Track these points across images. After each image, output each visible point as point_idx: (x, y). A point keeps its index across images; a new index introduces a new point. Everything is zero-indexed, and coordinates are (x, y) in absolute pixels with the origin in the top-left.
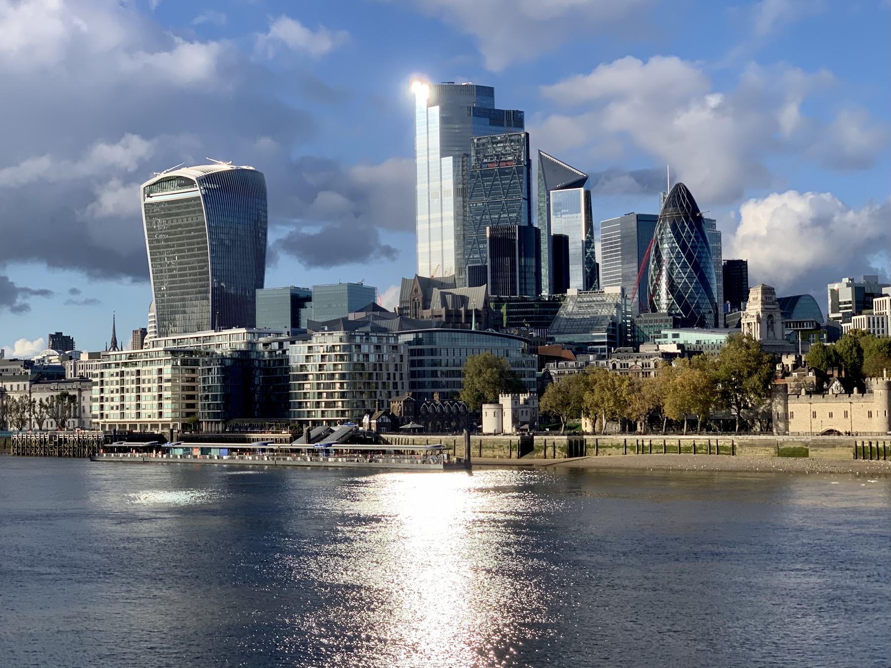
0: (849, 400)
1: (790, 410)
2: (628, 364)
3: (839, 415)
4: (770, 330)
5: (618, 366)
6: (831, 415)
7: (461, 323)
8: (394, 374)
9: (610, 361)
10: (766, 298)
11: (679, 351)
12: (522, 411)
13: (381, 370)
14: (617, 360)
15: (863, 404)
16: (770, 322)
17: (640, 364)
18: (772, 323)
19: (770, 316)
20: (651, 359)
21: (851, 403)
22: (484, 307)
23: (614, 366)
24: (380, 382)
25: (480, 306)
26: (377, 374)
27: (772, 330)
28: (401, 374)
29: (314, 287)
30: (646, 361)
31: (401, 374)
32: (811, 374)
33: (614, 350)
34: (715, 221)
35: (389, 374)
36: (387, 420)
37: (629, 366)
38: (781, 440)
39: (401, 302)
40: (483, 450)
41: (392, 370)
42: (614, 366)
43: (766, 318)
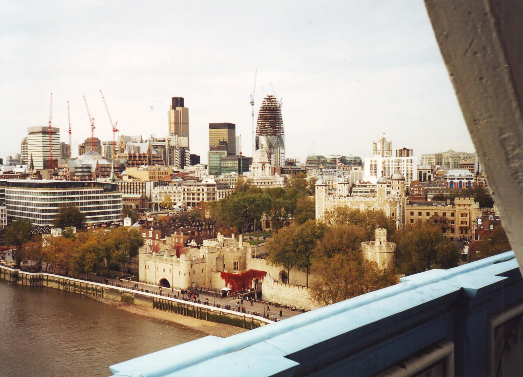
0: (171, 263)
3: (167, 271)
4: (263, 170)
5: (186, 190)
7: (136, 160)
9: (182, 187)
14: (186, 187)
17: (196, 189)
20: (201, 187)
21: (172, 265)
22: (148, 153)
23: (184, 190)
30: (198, 188)
37: (191, 190)
42: (184, 190)
43: (261, 166)
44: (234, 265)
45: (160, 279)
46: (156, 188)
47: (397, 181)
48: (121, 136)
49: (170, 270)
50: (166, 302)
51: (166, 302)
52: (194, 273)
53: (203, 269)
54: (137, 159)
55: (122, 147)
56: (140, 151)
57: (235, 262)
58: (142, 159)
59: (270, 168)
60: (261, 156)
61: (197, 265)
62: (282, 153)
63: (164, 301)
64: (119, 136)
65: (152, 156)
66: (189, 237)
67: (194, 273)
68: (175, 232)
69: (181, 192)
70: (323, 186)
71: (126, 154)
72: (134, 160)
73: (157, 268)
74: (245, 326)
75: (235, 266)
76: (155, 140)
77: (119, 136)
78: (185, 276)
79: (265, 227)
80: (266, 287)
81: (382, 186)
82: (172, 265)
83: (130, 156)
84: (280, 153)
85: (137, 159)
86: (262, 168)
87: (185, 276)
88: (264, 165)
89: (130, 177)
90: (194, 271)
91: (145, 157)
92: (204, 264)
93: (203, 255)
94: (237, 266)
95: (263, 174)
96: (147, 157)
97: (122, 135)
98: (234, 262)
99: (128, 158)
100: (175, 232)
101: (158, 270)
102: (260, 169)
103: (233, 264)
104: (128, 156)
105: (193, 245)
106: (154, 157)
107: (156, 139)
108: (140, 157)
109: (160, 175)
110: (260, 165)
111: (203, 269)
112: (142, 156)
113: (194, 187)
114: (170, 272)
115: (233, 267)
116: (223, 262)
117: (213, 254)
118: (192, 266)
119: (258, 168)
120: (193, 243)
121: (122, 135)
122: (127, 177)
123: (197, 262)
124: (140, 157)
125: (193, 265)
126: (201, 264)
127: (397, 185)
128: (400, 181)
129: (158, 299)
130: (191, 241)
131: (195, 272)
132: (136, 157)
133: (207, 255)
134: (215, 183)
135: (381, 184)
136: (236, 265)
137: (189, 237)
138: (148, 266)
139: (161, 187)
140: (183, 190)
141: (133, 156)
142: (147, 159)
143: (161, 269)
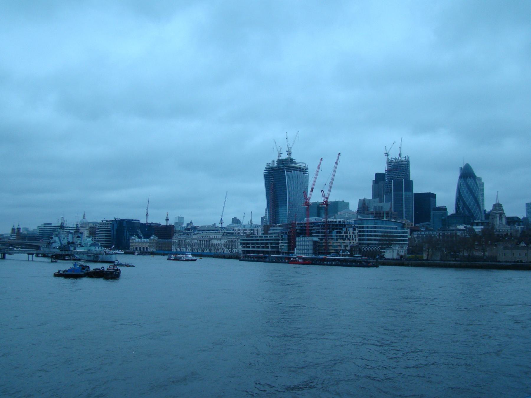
2: (444, 233)
5: (441, 234)
6: (520, 255)
8: (352, 236)
10: (499, 208)
11: (465, 228)
12: (401, 251)
13: (347, 233)
16: (500, 218)
17: (449, 233)
23: (439, 234)
25: (388, 210)
27: (502, 221)
28: (355, 236)
30: (452, 232)
31: (355, 236)
32: (513, 238)
34: (481, 178)
35: (350, 236)
36: (349, 253)
41: (351, 234)
42: (439, 234)
43: (499, 216)
46: (415, 233)
48: (363, 199)
49: (526, 254)
69: (437, 235)
71: (373, 212)
83: (376, 213)
86: (499, 218)
95: (501, 222)
97: (364, 198)
99: (374, 215)
100: (507, 238)
101: (513, 255)
102: (498, 219)
104: (374, 213)
109: (408, 226)
110: (498, 215)
113: (447, 231)
119: (496, 218)
120: (523, 244)
130: (520, 243)
132: (380, 214)
134: (465, 228)
138: (505, 254)
139: (419, 233)
140: (438, 234)
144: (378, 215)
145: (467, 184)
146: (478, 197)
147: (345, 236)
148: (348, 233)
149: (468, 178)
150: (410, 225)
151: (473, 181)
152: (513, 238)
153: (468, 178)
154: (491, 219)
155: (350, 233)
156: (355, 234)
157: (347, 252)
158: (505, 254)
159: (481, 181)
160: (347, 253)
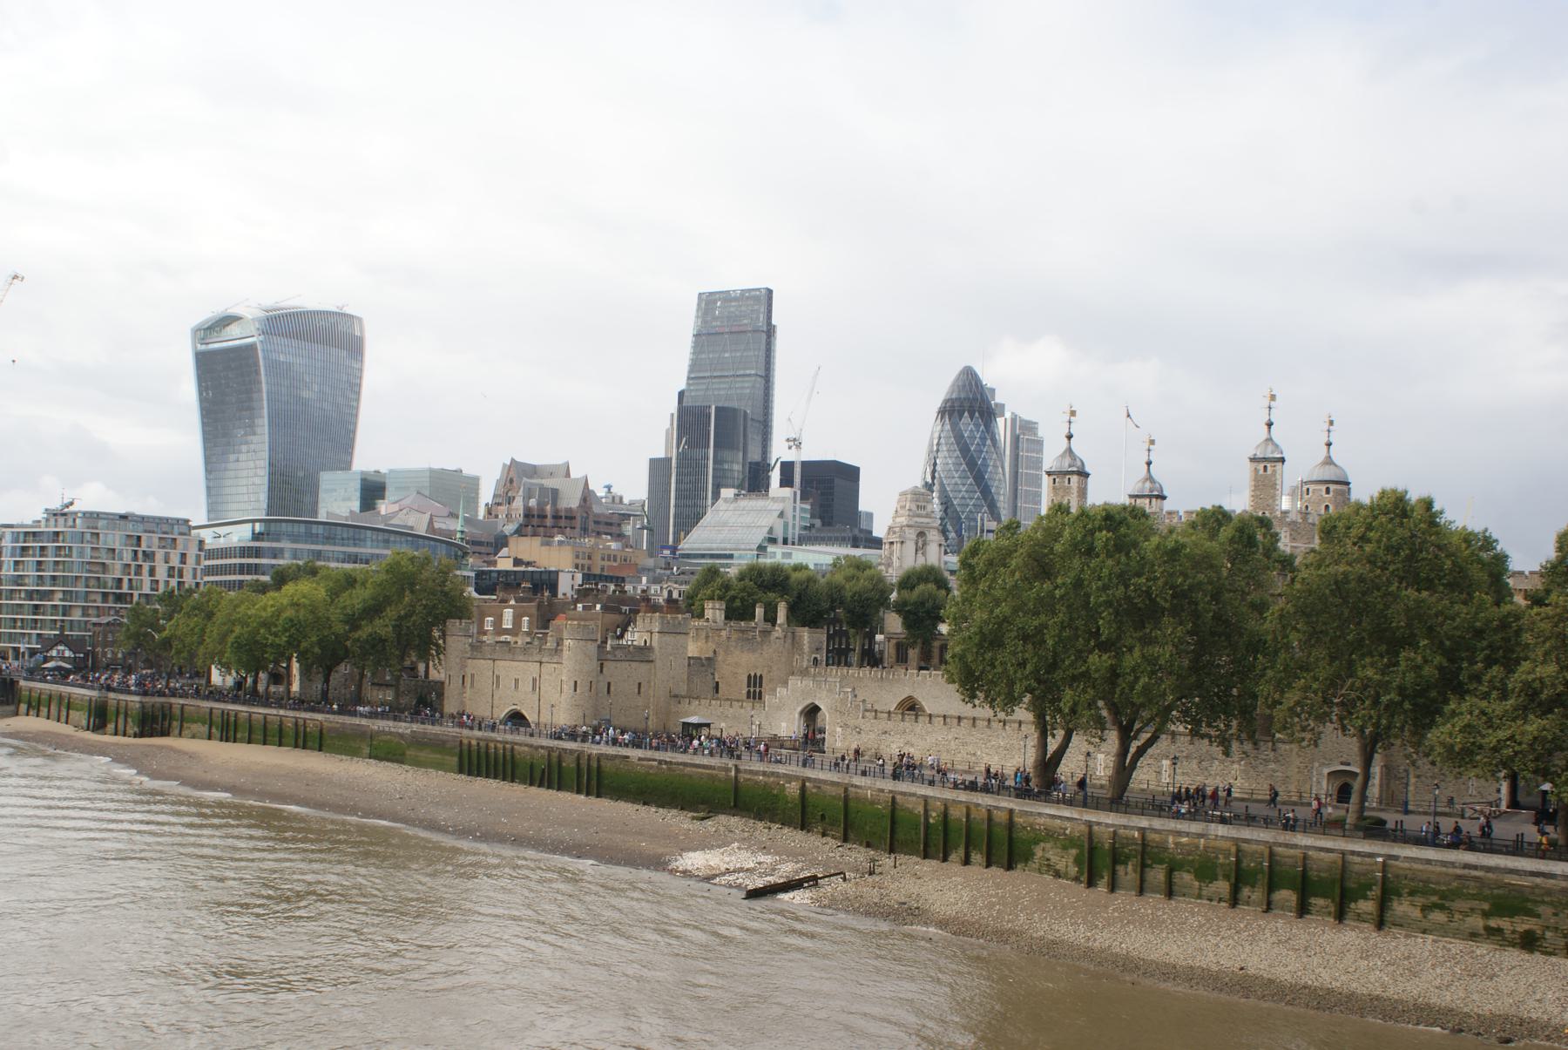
1: (469, 671)
3: (526, 686)
4: (920, 552)
7: (545, 527)
9: (665, 586)
14: (675, 586)
15: (555, 665)
16: (920, 544)
18: (924, 544)
19: (921, 534)
21: (541, 663)
22: (580, 506)
23: (670, 593)
24: (136, 594)
26: (130, 580)
29: (391, 471)
32: (598, 607)
33: (678, 569)
36: (68, 654)
38: (376, 728)
39: (495, 496)
40: (71, 712)
42: (670, 593)
43: (914, 537)
44: (749, 686)
45: (506, 711)
47: (1323, 488)
49: (534, 680)
50: (496, 748)
51: (496, 748)
52: (609, 692)
53: (640, 684)
54: (549, 522)
55: (510, 494)
56: (559, 501)
57: (753, 674)
58: (563, 523)
59: (940, 545)
60: (914, 508)
61: (619, 664)
62: (988, 531)
63: (492, 745)
64: (504, 465)
65: (591, 517)
66: (617, 618)
67: (609, 692)
68: (580, 606)
70: (1072, 473)
72: (538, 526)
73: (498, 677)
74: (735, 802)
75: (752, 690)
76: (617, 500)
77: (504, 465)
78: (575, 690)
79: (893, 659)
80: (839, 729)
81: (1269, 468)
82: (541, 663)
83: (528, 514)
84: (982, 531)
85: (549, 522)
86: (917, 544)
87: (575, 690)
88: (921, 534)
89: (517, 562)
90: (609, 684)
91: (572, 518)
92: (644, 667)
93: (646, 641)
94: (758, 690)
96: (579, 519)
97: (513, 460)
98: (749, 676)
100: (580, 606)
101: (498, 686)
102: (910, 547)
103: (746, 679)
105: (630, 643)
106: (597, 523)
107: (621, 498)
108: (556, 517)
109: (606, 563)
111: (640, 684)
112: (563, 514)
114: (534, 689)
115: (745, 692)
116: (713, 674)
117: (679, 637)
118: (602, 664)
121: (513, 460)
122: (511, 561)
123: (619, 654)
124: (556, 517)
125: (605, 663)
126: (634, 665)
127: (1321, 500)
128: (1332, 487)
129: (474, 742)
131: (612, 689)
132: (543, 517)
133: (656, 637)
135: (1265, 464)
136: (755, 686)
137: (617, 618)
138: (473, 675)
140: (665, 594)
141: (536, 513)
142: (578, 523)
143: (507, 684)
144: (535, 521)
145: (959, 437)
146: (996, 483)
147: (125, 584)
148: (146, 567)
149: (966, 414)
150: (615, 560)
151: (982, 427)
152: (598, 607)
153: (966, 414)
154: (887, 546)
155: (152, 572)
156: (181, 575)
157: (61, 648)
158: (473, 675)
159: (1036, 434)
160: (58, 651)
